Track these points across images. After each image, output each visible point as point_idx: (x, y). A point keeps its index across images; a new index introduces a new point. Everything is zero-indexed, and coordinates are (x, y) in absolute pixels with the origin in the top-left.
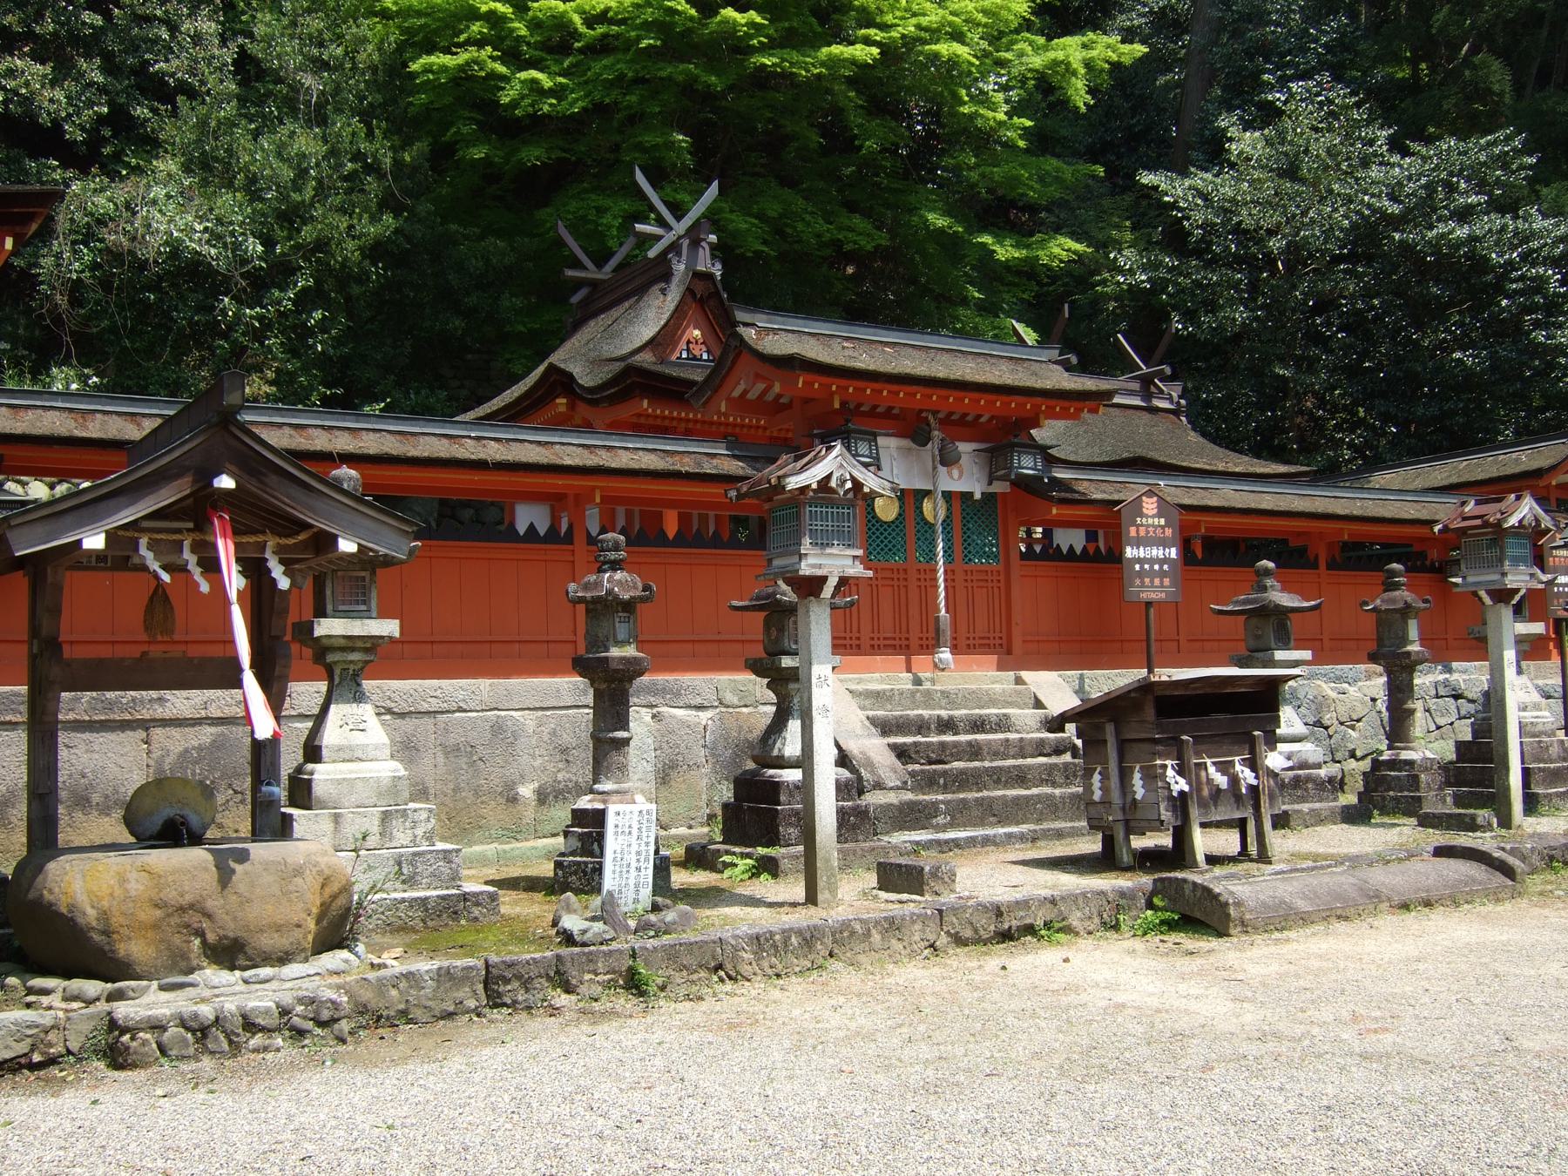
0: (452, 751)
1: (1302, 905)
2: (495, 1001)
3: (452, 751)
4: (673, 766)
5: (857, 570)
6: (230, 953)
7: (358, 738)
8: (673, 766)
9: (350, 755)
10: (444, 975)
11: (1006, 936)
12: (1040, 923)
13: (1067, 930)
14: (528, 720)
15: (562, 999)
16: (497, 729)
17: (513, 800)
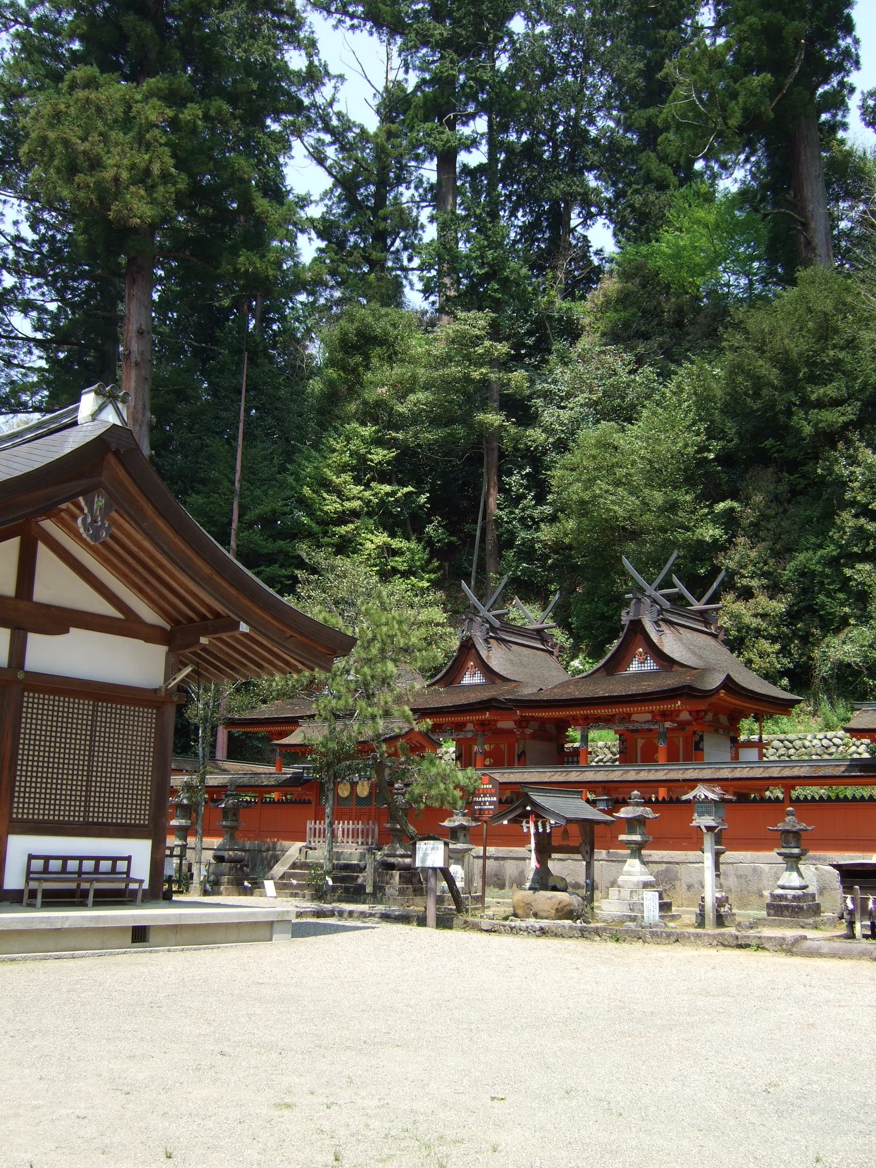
0: (739, 877)
1: (824, 950)
2: (583, 936)
3: (739, 877)
4: (825, 888)
5: (713, 824)
6: (536, 915)
7: (632, 869)
8: (825, 888)
9: (629, 874)
10: (571, 927)
11: (740, 946)
12: (754, 942)
13: (764, 948)
14: (766, 867)
15: (598, 938)
16: (755, 870)
17: (762, 896)
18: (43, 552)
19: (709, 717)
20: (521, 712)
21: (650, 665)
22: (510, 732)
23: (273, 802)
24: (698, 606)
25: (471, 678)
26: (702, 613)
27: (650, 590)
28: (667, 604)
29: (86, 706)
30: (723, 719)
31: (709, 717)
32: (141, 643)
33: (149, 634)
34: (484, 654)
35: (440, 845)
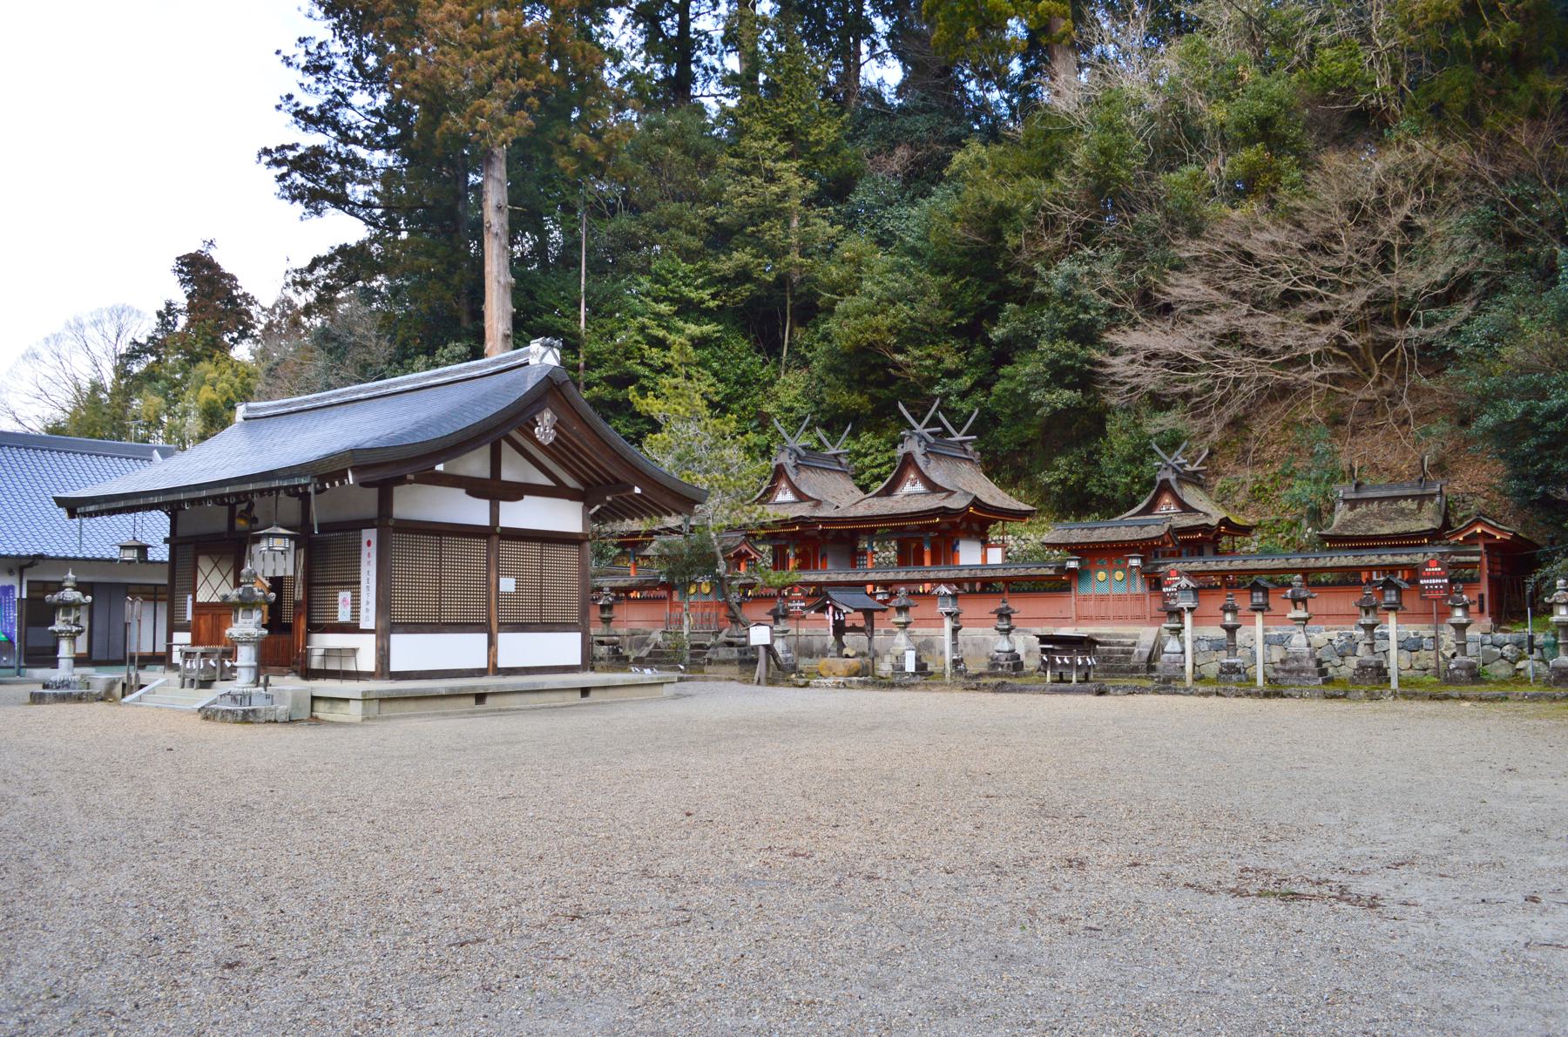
18: (506, 449)
19: (964, 526)
21: (920, 487)
23: (635, 599)
24: (958, 437)
25: (785, 496)
26: (961, 442)
27: (919, 429)
28: (932, 440)
29: (535, 548)
30: (976, 527)
31: (964, 526)
32: (566, 502)
33: (571, 495)
34: (793, 478)
35: (767, 629)
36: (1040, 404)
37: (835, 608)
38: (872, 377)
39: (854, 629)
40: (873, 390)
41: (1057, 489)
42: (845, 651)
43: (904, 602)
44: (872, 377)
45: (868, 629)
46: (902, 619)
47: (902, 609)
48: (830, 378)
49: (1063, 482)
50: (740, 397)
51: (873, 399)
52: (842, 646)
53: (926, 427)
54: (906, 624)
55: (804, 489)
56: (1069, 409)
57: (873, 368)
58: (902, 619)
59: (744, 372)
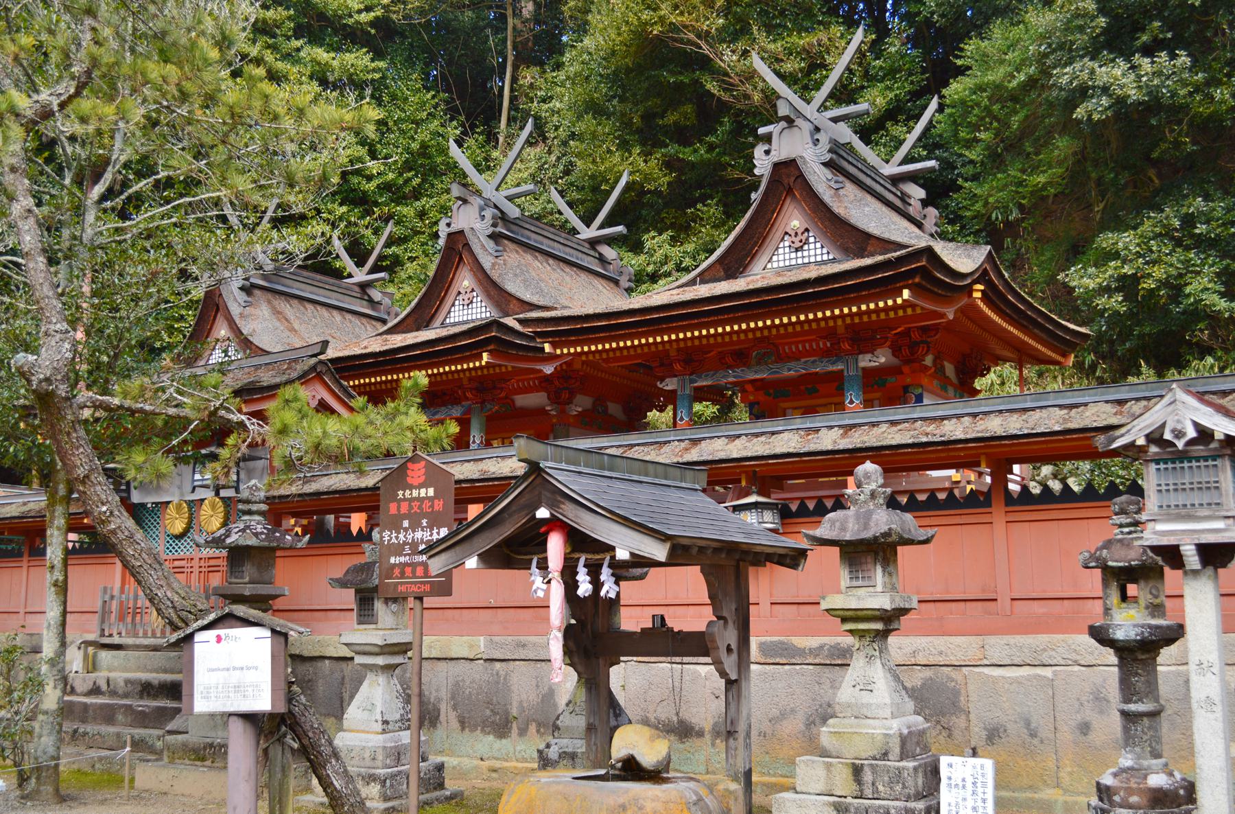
20: (554, 345)
22: (540, 412)
34: (486, 262)
36: (1083, 92)
37: (578, 541)
38: (671, 118)
39: (662, 641)
40: (672, 149)
41: (1116, 302)
42: (630, 741)
43: (882, 521)
44: (671, 118)
45: (722, 642)
46: (874, 594)
47: (865, 553)
48: (587, 124)
49: (1127, 285)
50: (417, 194)
51: (669, 164)
52: (605, 712)
53: (823, 107)
54: (890, 619)
55: (511, 287)
56: (1153, 105)
57: (675, 95)
58: (874, 594)
59: (424, 146)
